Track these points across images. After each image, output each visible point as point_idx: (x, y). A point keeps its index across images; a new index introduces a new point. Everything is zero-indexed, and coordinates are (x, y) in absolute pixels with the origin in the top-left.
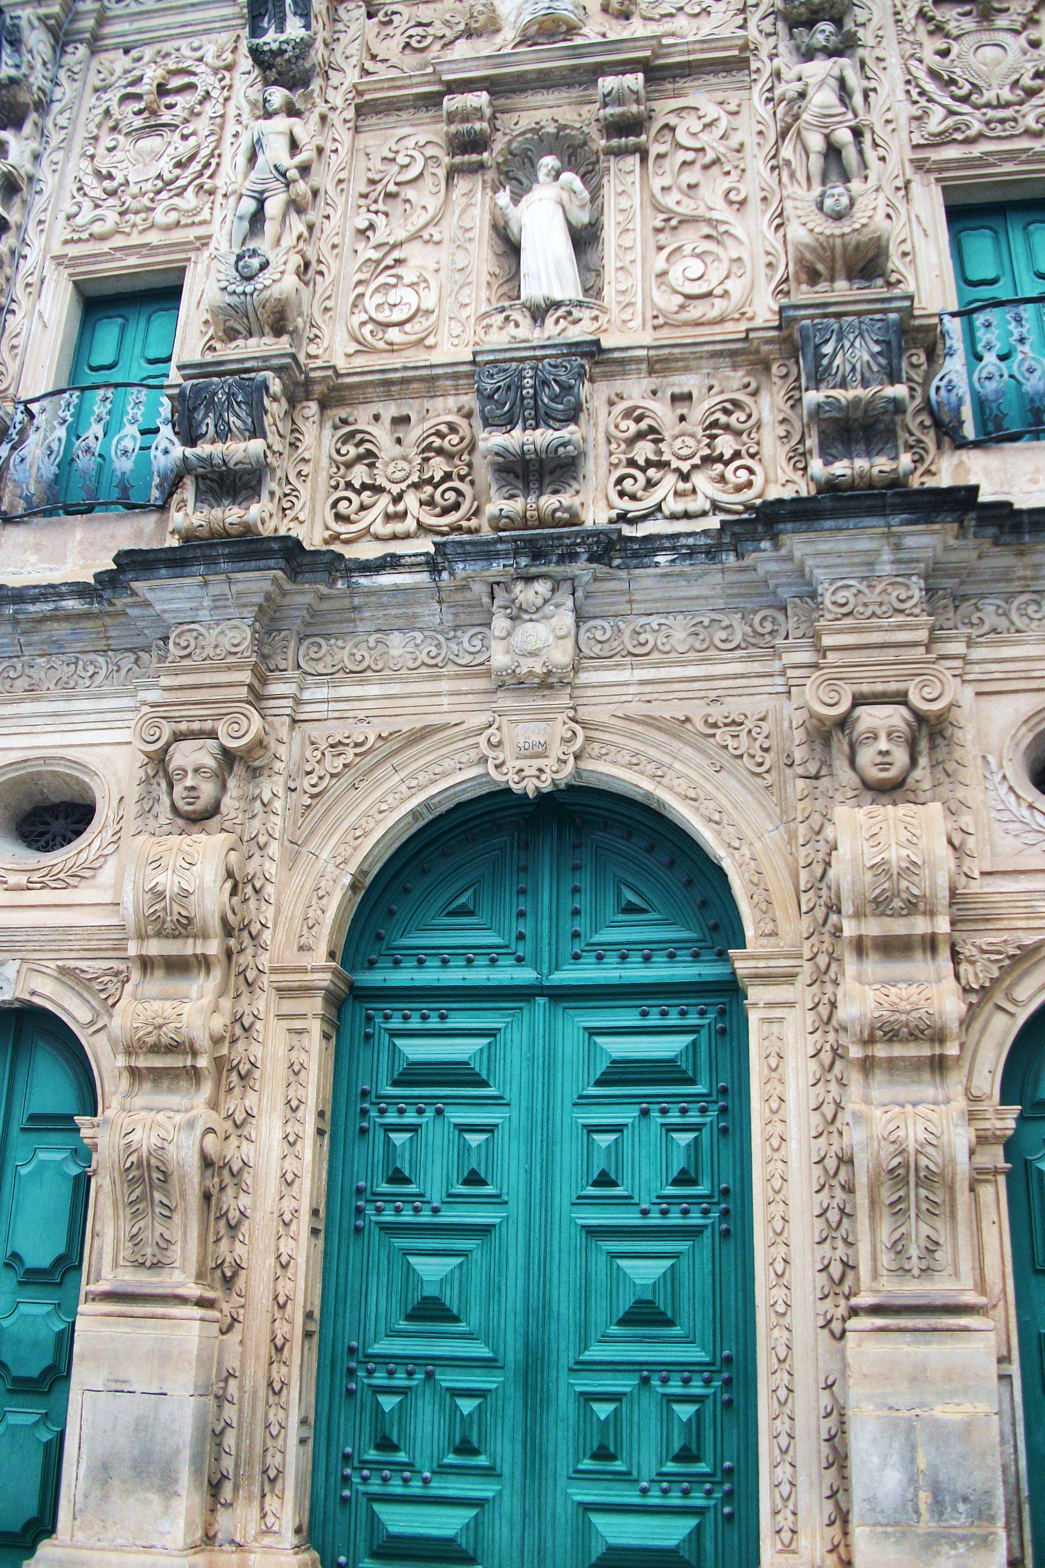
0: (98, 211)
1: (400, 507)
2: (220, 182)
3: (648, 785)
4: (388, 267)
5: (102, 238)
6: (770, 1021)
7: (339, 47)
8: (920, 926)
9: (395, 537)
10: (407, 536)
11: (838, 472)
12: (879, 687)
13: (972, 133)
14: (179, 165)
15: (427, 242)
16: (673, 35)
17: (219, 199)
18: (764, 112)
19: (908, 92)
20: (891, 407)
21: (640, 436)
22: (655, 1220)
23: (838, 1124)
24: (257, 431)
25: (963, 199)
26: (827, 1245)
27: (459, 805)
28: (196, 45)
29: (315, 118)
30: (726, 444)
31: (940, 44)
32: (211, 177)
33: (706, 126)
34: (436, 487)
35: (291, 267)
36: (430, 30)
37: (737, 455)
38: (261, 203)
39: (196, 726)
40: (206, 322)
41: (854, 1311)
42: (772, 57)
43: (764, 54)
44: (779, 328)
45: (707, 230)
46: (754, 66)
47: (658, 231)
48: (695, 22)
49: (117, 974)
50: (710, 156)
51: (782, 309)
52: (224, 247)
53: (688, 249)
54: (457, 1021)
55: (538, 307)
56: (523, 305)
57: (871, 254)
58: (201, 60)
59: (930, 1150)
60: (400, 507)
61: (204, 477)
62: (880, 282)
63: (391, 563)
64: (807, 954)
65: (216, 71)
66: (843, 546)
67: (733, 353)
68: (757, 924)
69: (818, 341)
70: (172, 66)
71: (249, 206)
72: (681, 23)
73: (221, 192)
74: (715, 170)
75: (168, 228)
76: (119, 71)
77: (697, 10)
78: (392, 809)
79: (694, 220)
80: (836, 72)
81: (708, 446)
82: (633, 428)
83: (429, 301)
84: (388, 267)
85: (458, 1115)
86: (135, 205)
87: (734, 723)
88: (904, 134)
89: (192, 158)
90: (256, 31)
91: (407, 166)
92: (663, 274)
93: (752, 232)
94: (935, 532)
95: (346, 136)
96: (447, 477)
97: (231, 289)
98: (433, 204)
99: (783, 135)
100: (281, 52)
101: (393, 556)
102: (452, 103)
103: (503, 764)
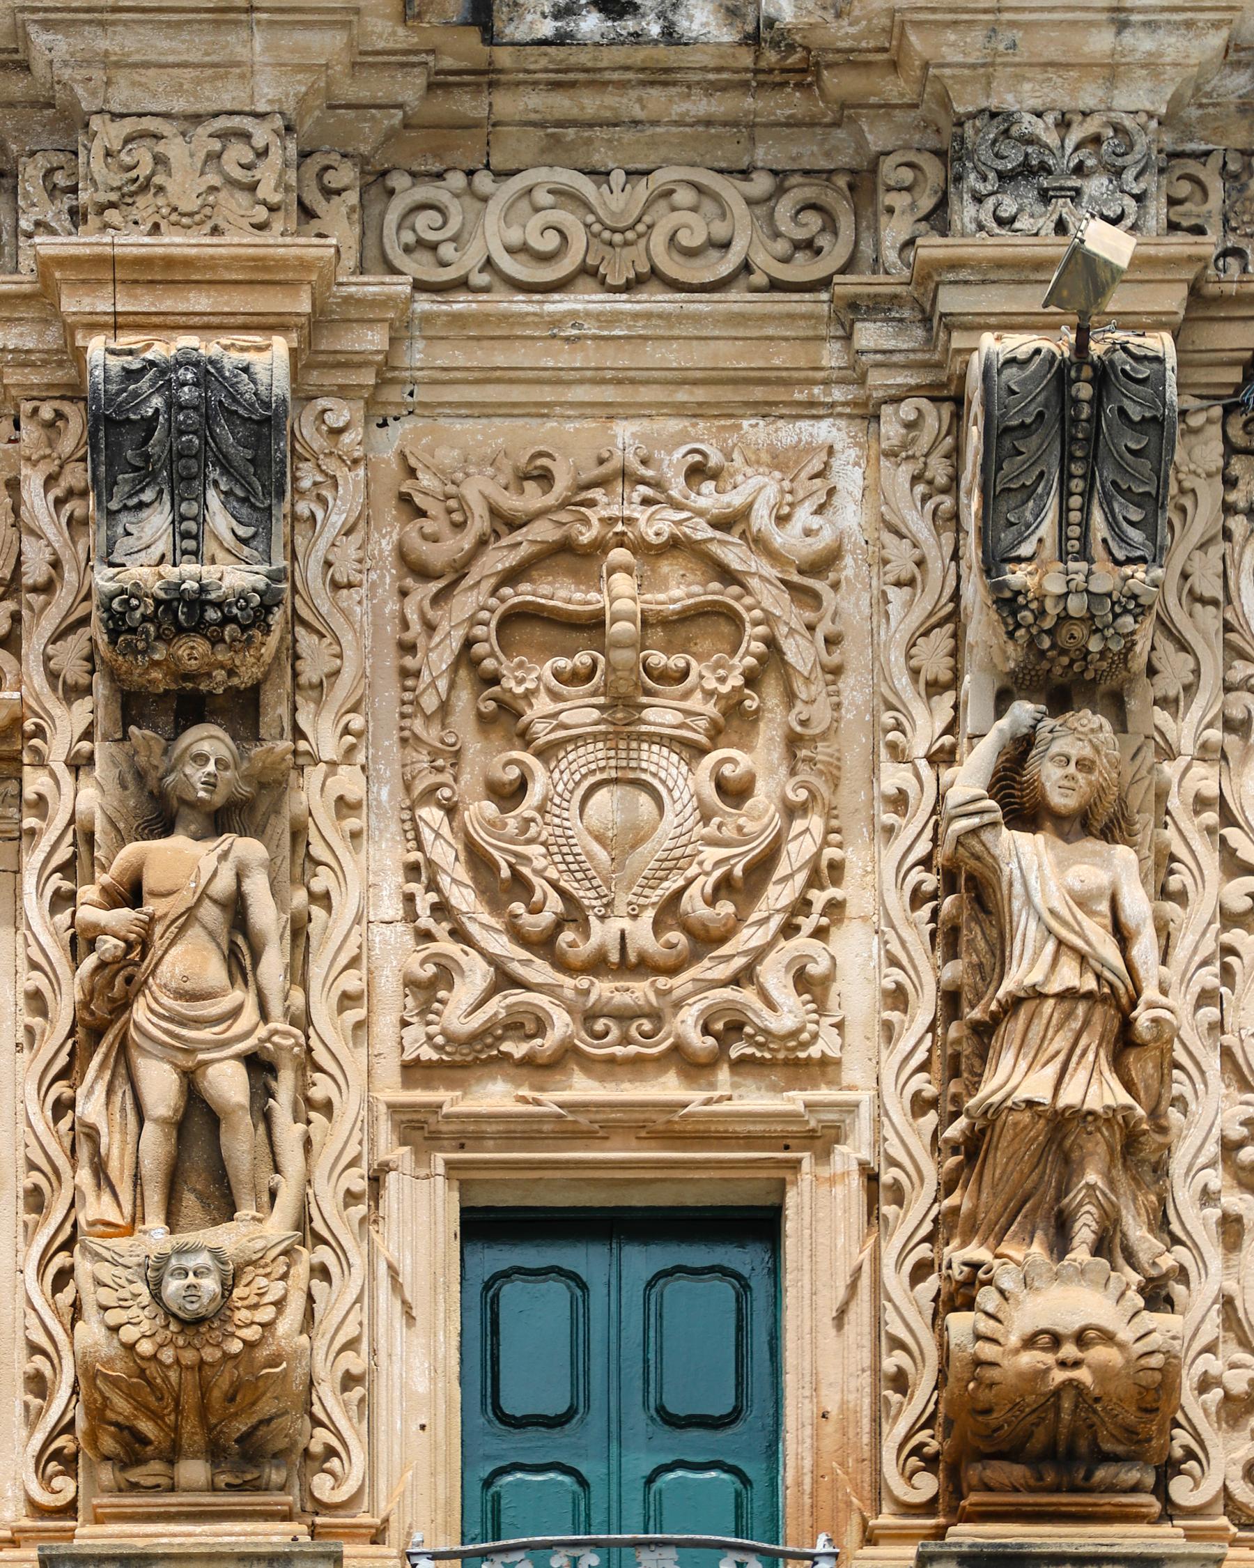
13: (548, 1043)
19: (410, 899)
31: (504, 761)
43: (57, 750)
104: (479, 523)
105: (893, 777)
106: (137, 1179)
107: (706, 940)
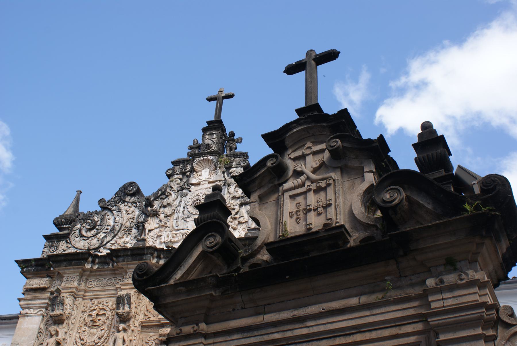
7: (139, 308)
29: (130, 331)
58: (107, 306)
76: (88, 307)
89: (102, 337)
90: (118, 308)
95: (138, 336)
100: (123, 315)
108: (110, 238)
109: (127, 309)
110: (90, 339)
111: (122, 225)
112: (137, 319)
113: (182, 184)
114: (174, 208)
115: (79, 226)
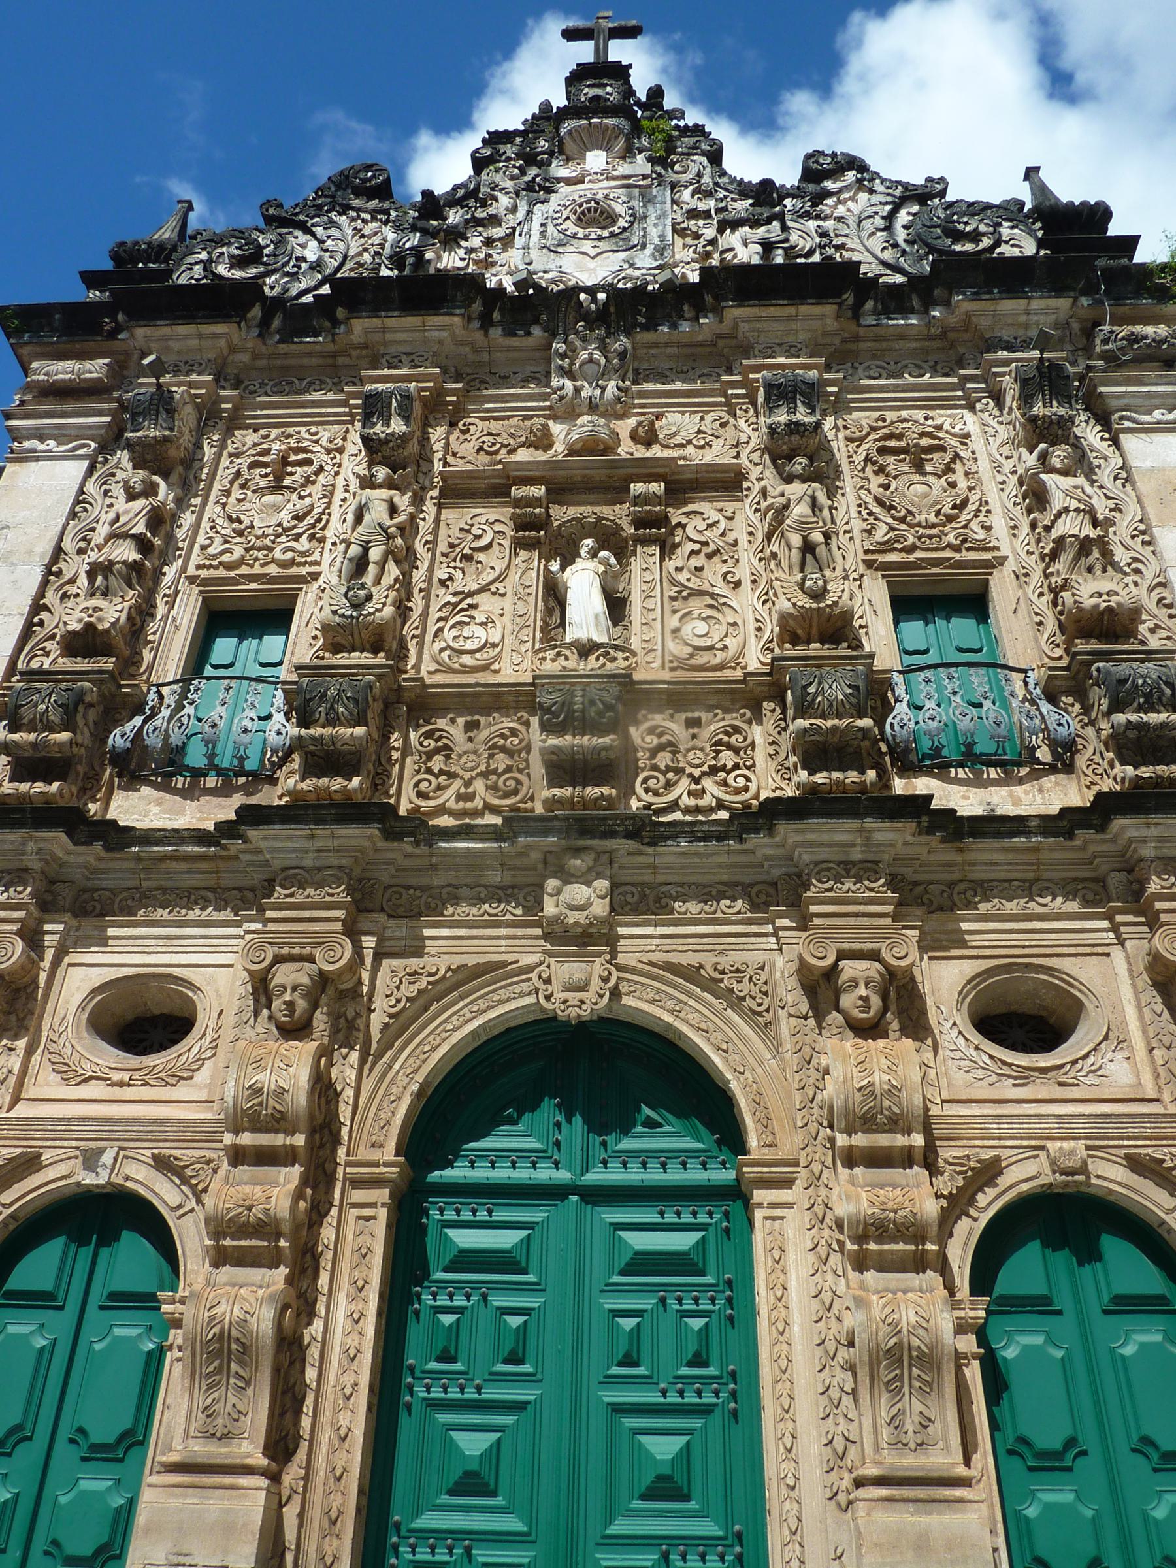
0: (227, 546)
1: (470, 790)
2: (329, 533)
3: (668, 1018)
4: (462, 610)
5: (229, 566)
6: (773, 1219)
8: (900, 1140)
9: (465, 813)
10: (476, 813)
11: (820, 781)
12: (857, 946)
13: (909, 542)
14: (299, 518)
15: (494, 594)
16: (684, 458)
17: (328, 546)
18: (755, 518)
20: (860, 735)
21: (661, 748)
22: (673, 1398)
23: (835, 1310)
24: (360, 721)
25: (899, 592)
26: (830, 1420)
27: (509, 1030)
28: (314, 429)
30: (727, 758)
31: (882, 479)
32: (323, 529)
33: (709, 526)
34: (500, 776)
35: (389, 601)
36: (499, 439)
37: (736, 767)
38: (366, 550)
39: (296, 951)
40: (315, 637)
41: (859, 1483)
42: (759, 479)
43: (753, 477)
44: (769, 674)
45: (709, 601)
46: (745, 485)
47: (673, 599)
48: (701, 452)
49: (209, 1162)
50: (712, 547)
51: (774, 659)
52: (334, 580)
53: (696, 614)
54: (500, 1215)
55: (584, 645)
56: (572, 644)
57: (839, 624)
58: (317, 442)
59: (921, 1332)
60: (470, 790)
61: (312, 754)
62: (845, 645)
63: (465, 832)
64: (803, 1163)
65: (328, 451)
66: (825, 838)
67: (733, 692)
68: (759, 1136)
69: (804, 683)
70: (293, 445)
71: (355, 550)
72: (690, 450)
73: (329, 542)
74: (716, 559)
75: (284, 565)
76: (250, 443)
77: (702, 442)
78: (455, 1029)
79: (701, 593)
80: (810, 492)
81: (715, 758)
82: (656, 741)
83: (496, 640)
84: (462, 610)
85: (498, 1300)
86: (259, 543)
87: (738, 971)
88: (858, 541)
91: (479, 537)
92: (676, 631)
93: (746, 603)
94: (898, 830)
96: (509, 769)
97: (341, 612)
98: (500, 566)
99: (769, 536)
100: (387, 441)
101: (468, 825)
102: (516, 492)
103: (552, 995)
104: (866, 430)
105: (1000, 478)
106: (790, 567)
107: (950, 519)
108: (313, 283)
109: (397, 426)
110: (262, 520)
111: (345, 257)
112: (424, 469)
113: (527, 178)
114: (511, 224)
115: (204, 256)
